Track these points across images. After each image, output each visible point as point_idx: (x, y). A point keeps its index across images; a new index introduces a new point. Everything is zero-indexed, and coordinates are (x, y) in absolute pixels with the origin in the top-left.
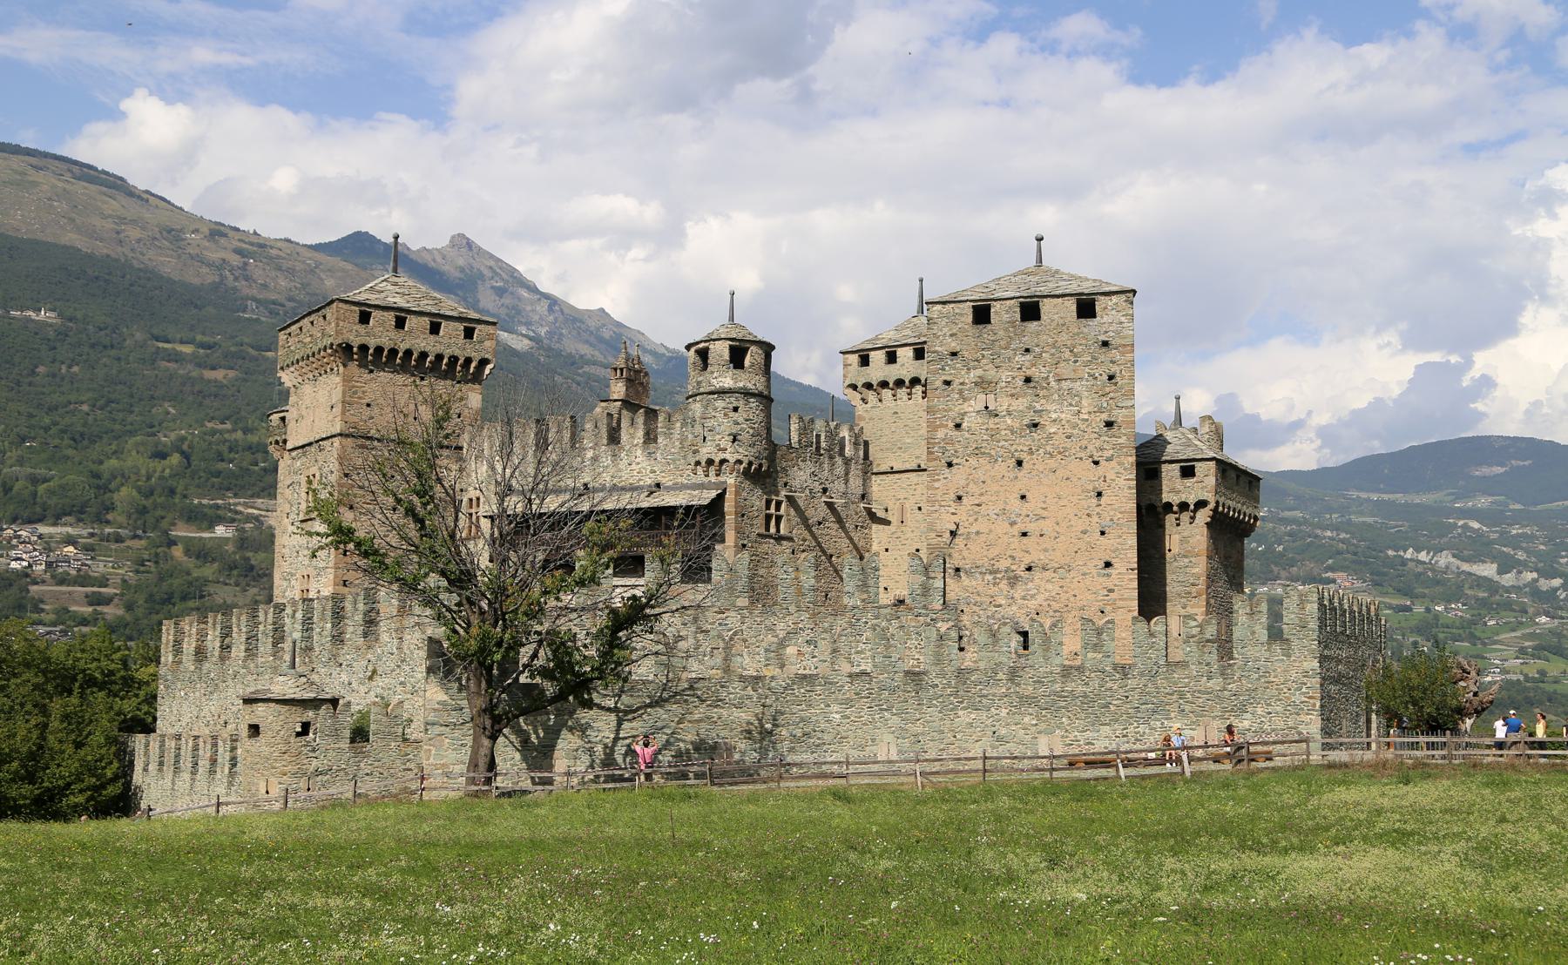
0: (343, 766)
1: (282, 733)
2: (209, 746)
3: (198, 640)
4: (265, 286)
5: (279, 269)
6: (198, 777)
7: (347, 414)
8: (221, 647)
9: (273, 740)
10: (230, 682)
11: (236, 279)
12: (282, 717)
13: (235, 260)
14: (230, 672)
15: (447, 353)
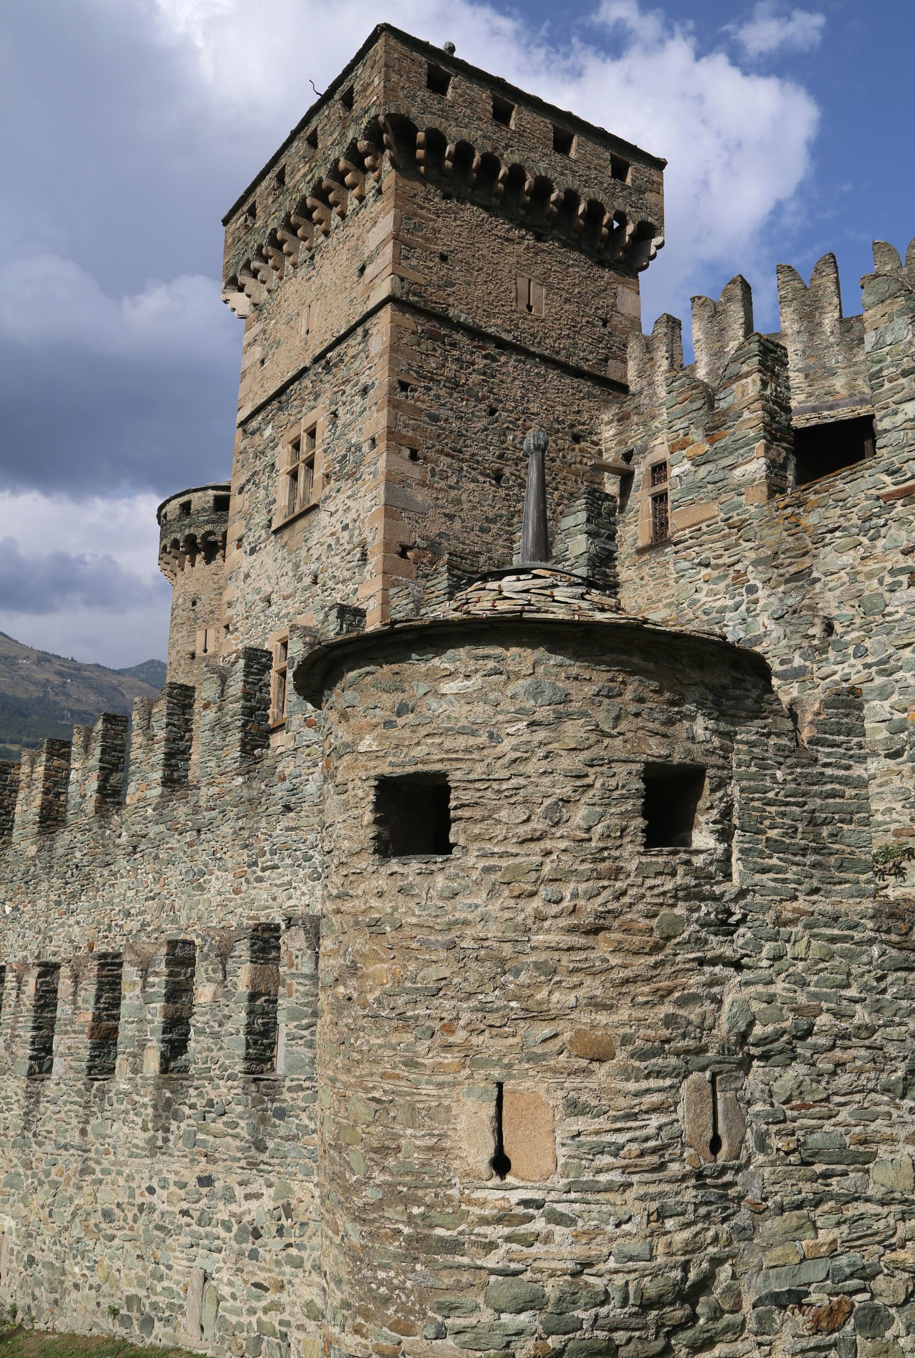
0: (862, 1015)
1: (579, 815)
2: (89, 989)
3: (46, 792)
4: (78, 700)
5: (90, 687)
6: (51, 1088)
7: (404, 263)
8: (101, 790)
9: (531, 855)
10: (122, 864)
11: (57, 694)
12: (574, 731)
13: (56, 680)
14: (124, 839)
15: (587, 193)
